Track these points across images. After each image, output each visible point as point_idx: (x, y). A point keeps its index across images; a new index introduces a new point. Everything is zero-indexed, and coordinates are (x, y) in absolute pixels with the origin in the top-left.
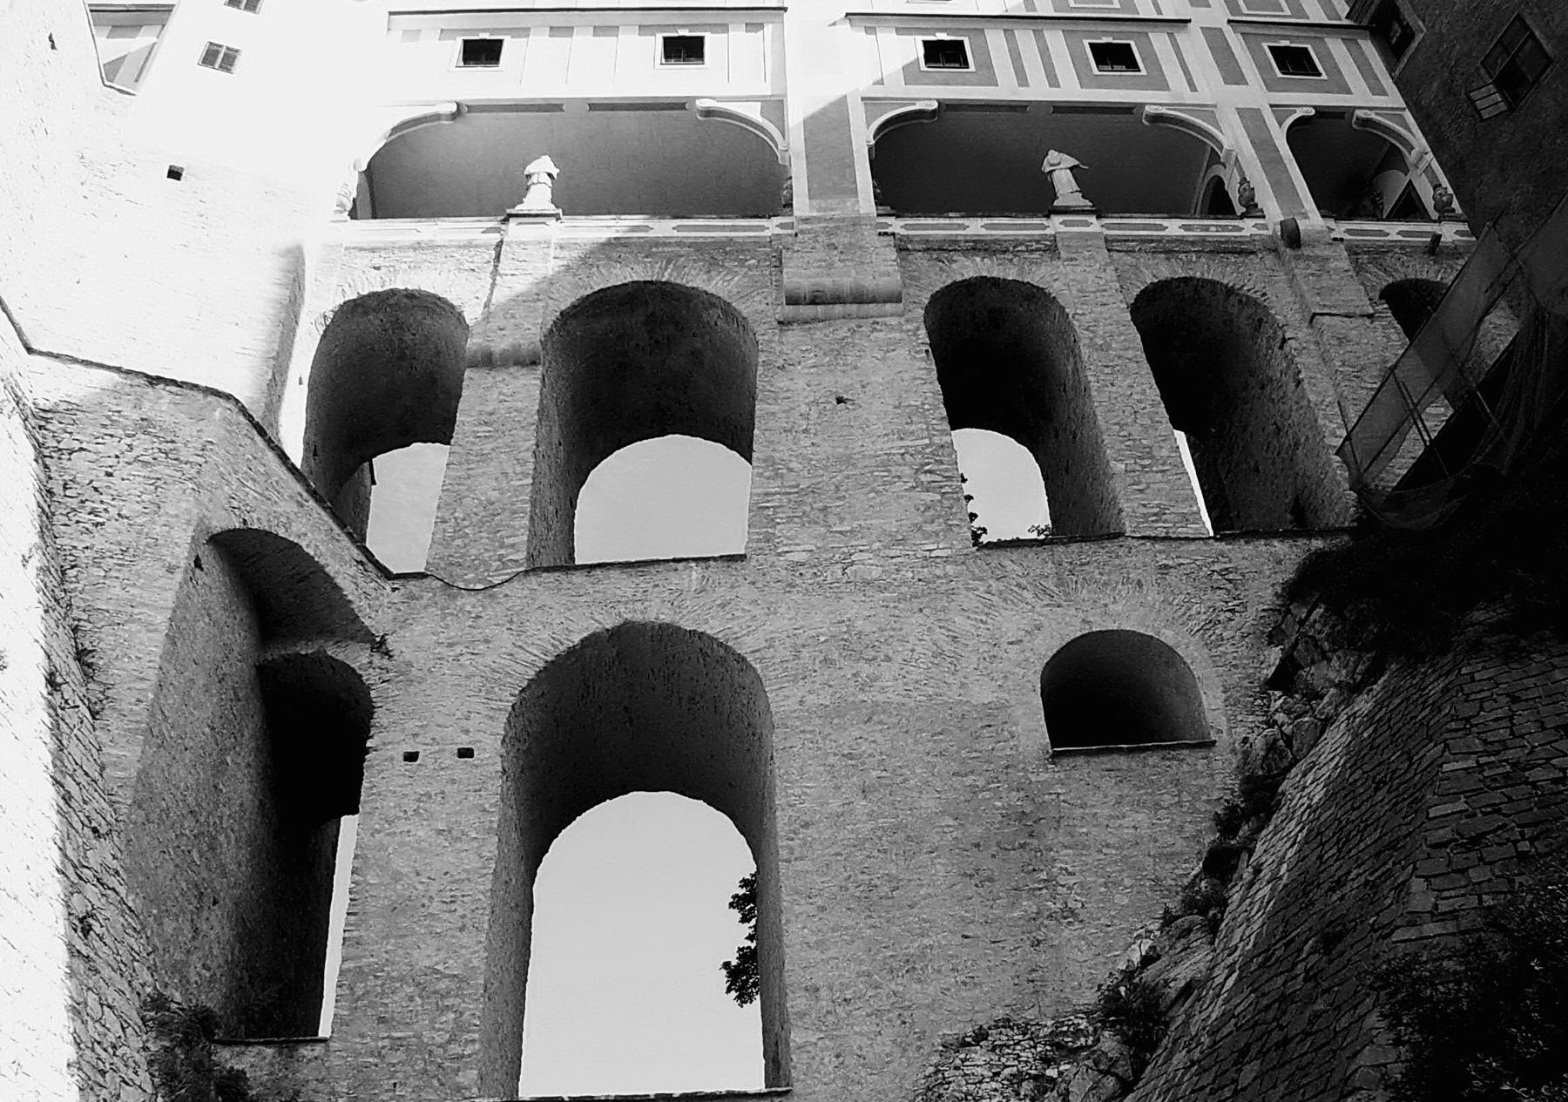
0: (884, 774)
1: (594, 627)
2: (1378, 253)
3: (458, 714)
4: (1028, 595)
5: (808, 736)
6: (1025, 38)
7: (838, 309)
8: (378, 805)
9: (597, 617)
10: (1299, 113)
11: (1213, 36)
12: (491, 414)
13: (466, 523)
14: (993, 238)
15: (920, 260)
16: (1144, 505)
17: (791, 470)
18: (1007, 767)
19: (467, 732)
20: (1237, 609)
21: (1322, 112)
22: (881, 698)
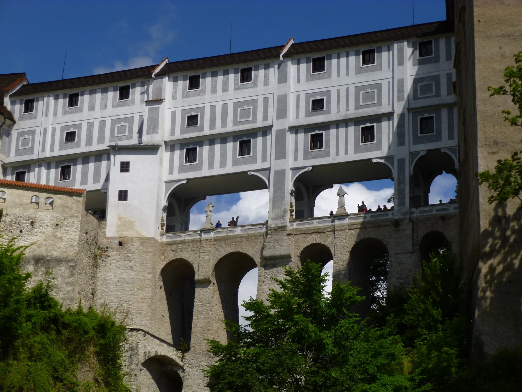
12: (202, 299)
13: (198, 333)
14: (318, 228)
21: (428, 151)
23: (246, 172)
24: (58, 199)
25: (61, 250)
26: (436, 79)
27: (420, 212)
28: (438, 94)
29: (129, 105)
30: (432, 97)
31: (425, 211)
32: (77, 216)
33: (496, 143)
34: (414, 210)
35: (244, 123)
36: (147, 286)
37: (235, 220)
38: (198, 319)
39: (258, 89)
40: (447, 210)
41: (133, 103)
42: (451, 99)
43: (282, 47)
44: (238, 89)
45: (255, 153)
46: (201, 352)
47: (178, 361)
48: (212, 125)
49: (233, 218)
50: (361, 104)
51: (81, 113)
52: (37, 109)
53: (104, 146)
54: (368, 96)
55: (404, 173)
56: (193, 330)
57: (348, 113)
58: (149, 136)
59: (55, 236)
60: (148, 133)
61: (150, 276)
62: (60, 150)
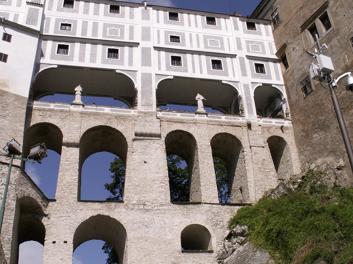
0: (149, 253)
1: (92, 215)
2: (269, 128)
3: (64, 233)
4: (180, 215)
5: (134, 243)
6: (196, 56)
8: (48, 253)
9: (93, 213)
10: (258, 85)
11: (241, 59)
12: (68, 159)
13: (64, 187)
15: (164, 124)
16: (206, 194)
17: (134, 180)
18: (173, 253)
19: (66, 237)
20: (222, 221)
21: (264, 84)
22: (150, 236)
27: (263, 121)
34: (259, 119)
35: (112, 37)
36: (19, 135)
38: (64, 175)
44: (107, 16)
45: (122, 59)
46: (68, 203)
54: (212, 42)
55: (250, 94)
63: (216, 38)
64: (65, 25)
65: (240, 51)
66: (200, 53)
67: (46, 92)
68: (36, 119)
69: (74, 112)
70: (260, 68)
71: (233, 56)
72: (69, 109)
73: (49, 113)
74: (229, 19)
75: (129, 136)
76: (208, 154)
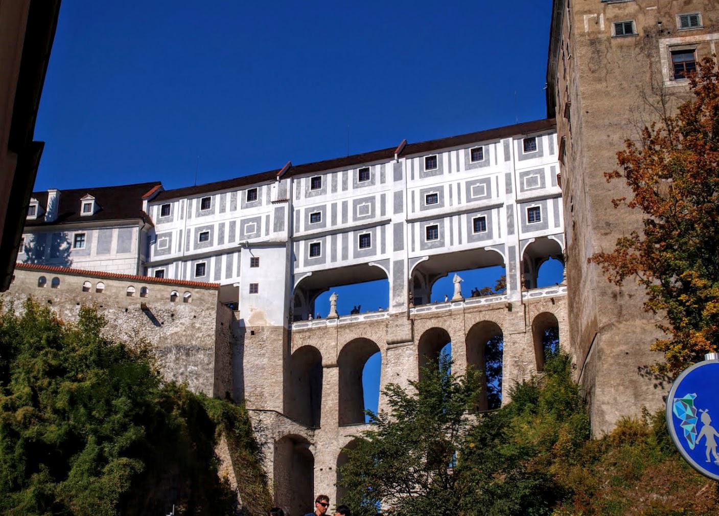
7: (399, 345)
10: (530, 241)
11: (510, 207)
21: (536, 238)
23: (367, 264)
24: (195, 293)
25: (199, 339)
26: (541, 172)
27: (531, 295)
28: (543, 186)
29: (256, 206)
30: (538, 188)
31: (535, 294)
32: (213, 308)
33: (608, 224)
35: (363, 218)
37: (357, 308)
39: (375, 186)
40: (556, 292)
41: (260, 203)
42: (557, 190)
43: (397, 148)
44: (357, 187)
45: (375, 247)
47: (309, 439)
48: (334, 222)
49: (355, 307)
50: (472, 197)
51: (213, 215)
52: (172, 213)
53: (235, 244)
56: (322, 411)
57: (460, 205)
58: (276, 233)
59: (194, 327)
60: (275, 231)
61: (281, 362)
62: (195, 249)
63: (482, 181)
64: (316, 217)
65: (509, 195)
66: (459, 213)
67: (321, 289)
68: (297, 343)
69: (330, 328)
70: (534, 215)
71: (499, 206)
72: (324, 325)
73: (308, 334)
74: (499, 142)
75: (383, 346)
76: (462, 353)
